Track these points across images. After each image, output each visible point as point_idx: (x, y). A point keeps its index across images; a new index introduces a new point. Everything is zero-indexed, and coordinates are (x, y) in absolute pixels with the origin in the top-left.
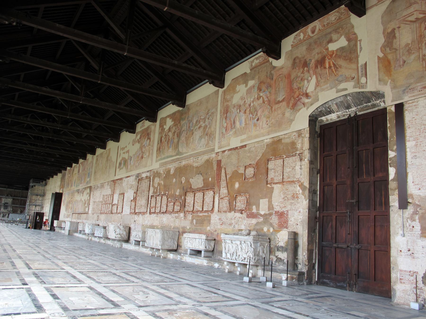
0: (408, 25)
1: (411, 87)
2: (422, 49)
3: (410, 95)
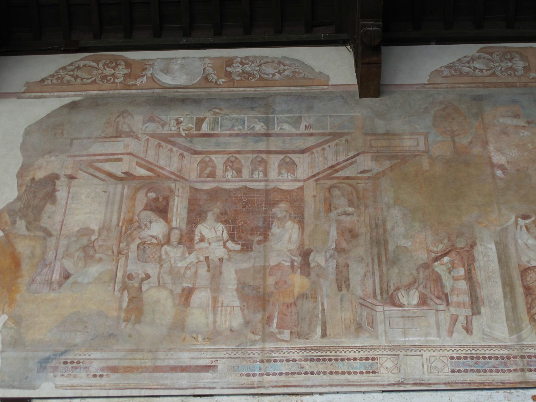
0: (102, 183)
1: (69, 356)
2: (127, 257)
3: (60, 381)
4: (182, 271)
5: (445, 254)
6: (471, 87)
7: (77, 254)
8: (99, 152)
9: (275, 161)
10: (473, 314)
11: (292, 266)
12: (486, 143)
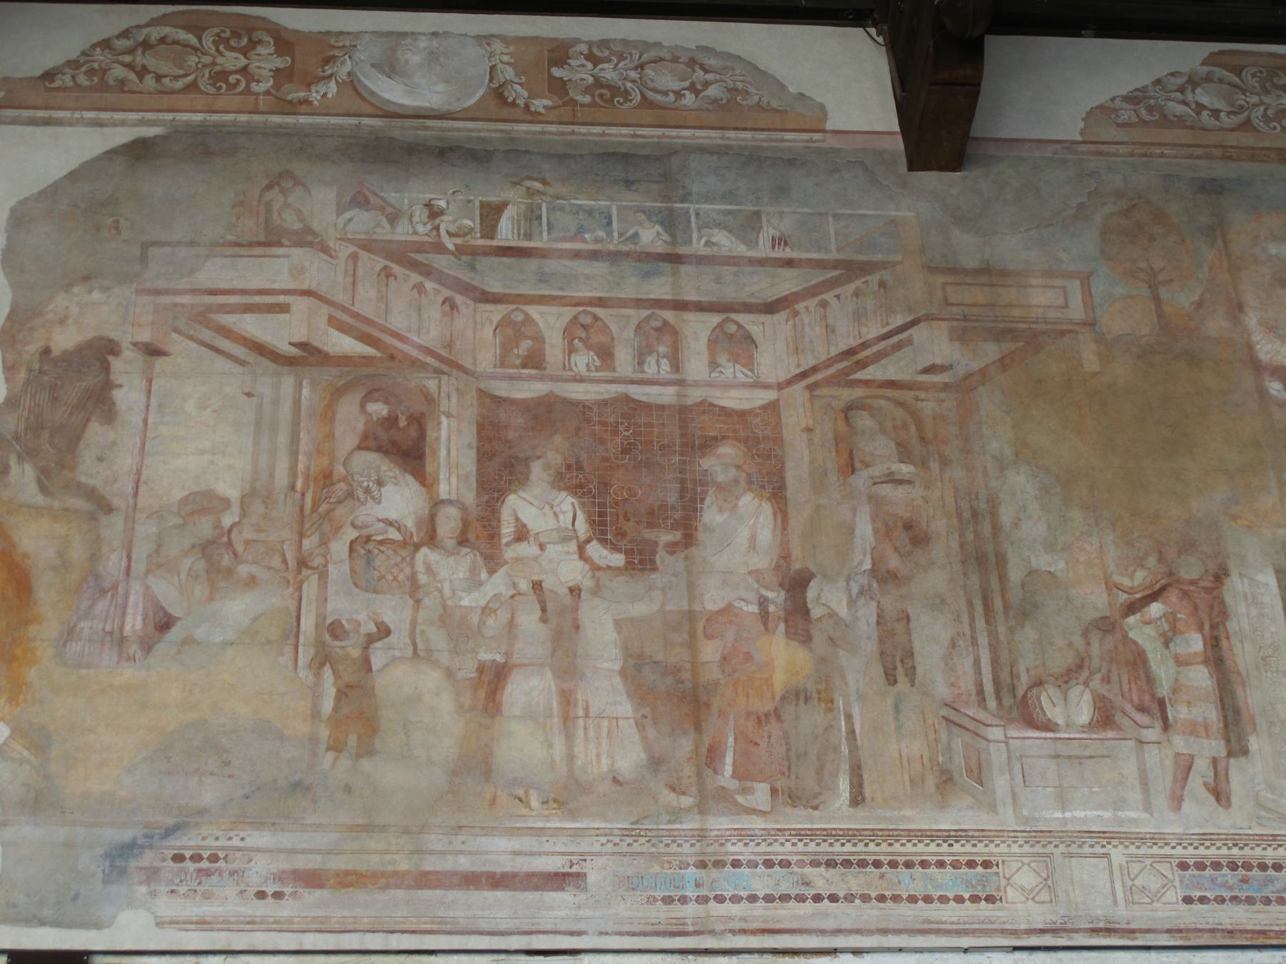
0: (238, 369)
1: (188, 842)
2: (323, 576)
3: (167, 907)
4: (475, 618)
5: (1153, 597)
6: (1190, 157)
7: (186, 564)
8: (222, 286)
9: (699, 328)
11: (764, 615)
12: (1237, 309)
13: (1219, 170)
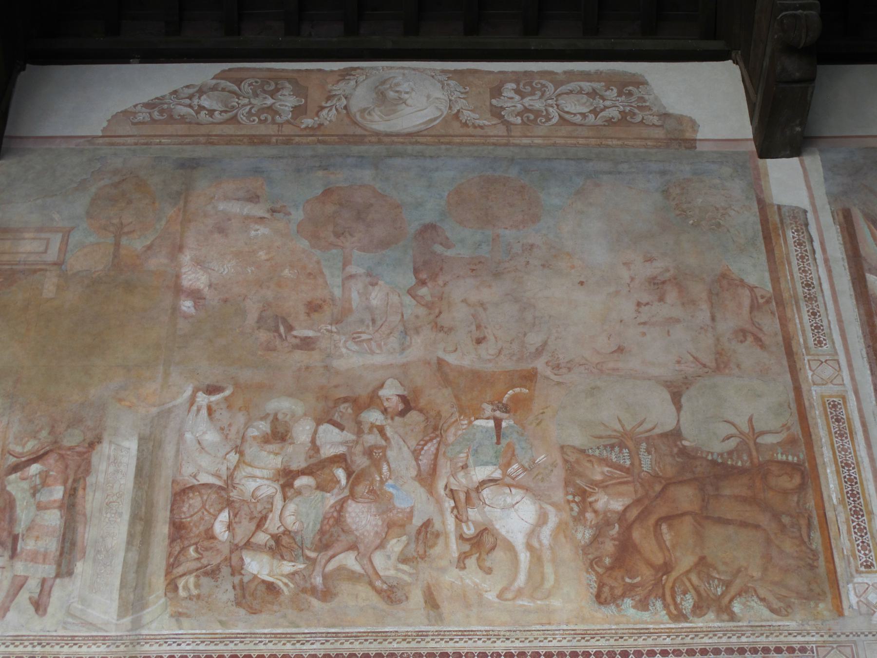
10: (58, 575)
13: (200, 152)
